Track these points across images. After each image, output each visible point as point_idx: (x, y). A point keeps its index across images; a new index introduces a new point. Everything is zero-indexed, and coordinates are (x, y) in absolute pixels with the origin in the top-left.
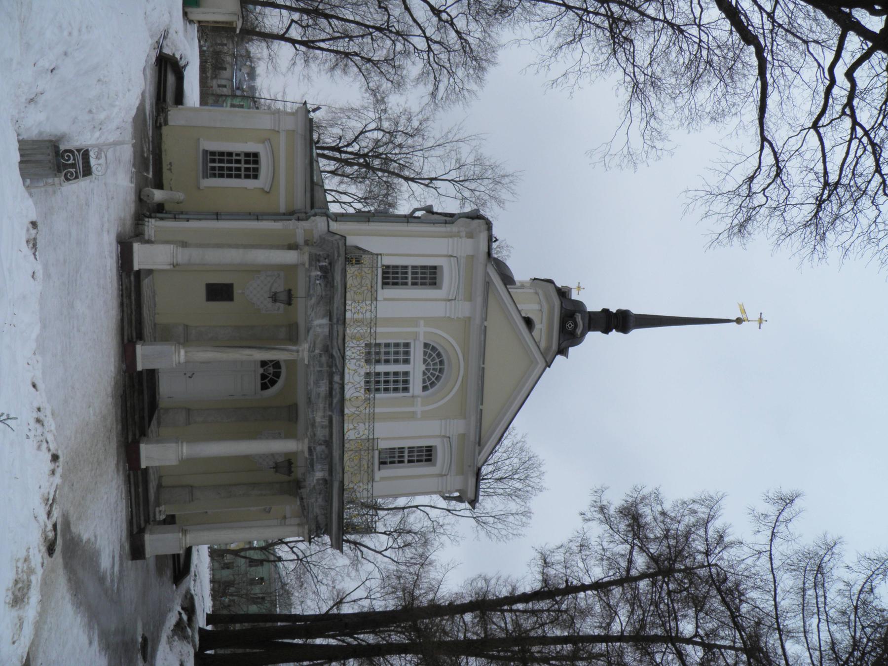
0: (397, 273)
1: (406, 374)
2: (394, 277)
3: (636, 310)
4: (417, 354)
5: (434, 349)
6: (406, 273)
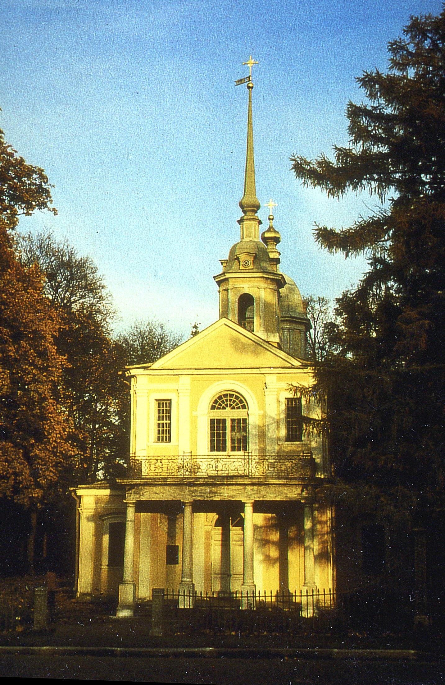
0: (163, 430)
1: (233, 420)
2: (164, 434)
3: (239, 195)
4: (219, 414)
5: (216, 402)
6: (163, 424)
